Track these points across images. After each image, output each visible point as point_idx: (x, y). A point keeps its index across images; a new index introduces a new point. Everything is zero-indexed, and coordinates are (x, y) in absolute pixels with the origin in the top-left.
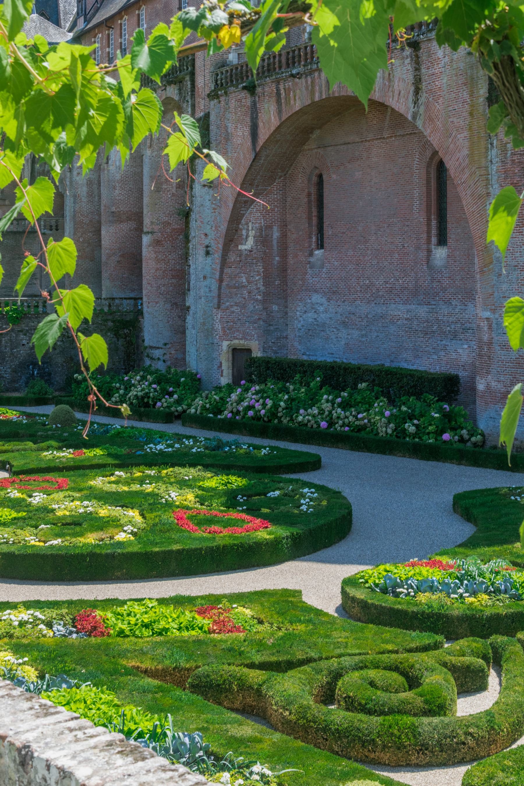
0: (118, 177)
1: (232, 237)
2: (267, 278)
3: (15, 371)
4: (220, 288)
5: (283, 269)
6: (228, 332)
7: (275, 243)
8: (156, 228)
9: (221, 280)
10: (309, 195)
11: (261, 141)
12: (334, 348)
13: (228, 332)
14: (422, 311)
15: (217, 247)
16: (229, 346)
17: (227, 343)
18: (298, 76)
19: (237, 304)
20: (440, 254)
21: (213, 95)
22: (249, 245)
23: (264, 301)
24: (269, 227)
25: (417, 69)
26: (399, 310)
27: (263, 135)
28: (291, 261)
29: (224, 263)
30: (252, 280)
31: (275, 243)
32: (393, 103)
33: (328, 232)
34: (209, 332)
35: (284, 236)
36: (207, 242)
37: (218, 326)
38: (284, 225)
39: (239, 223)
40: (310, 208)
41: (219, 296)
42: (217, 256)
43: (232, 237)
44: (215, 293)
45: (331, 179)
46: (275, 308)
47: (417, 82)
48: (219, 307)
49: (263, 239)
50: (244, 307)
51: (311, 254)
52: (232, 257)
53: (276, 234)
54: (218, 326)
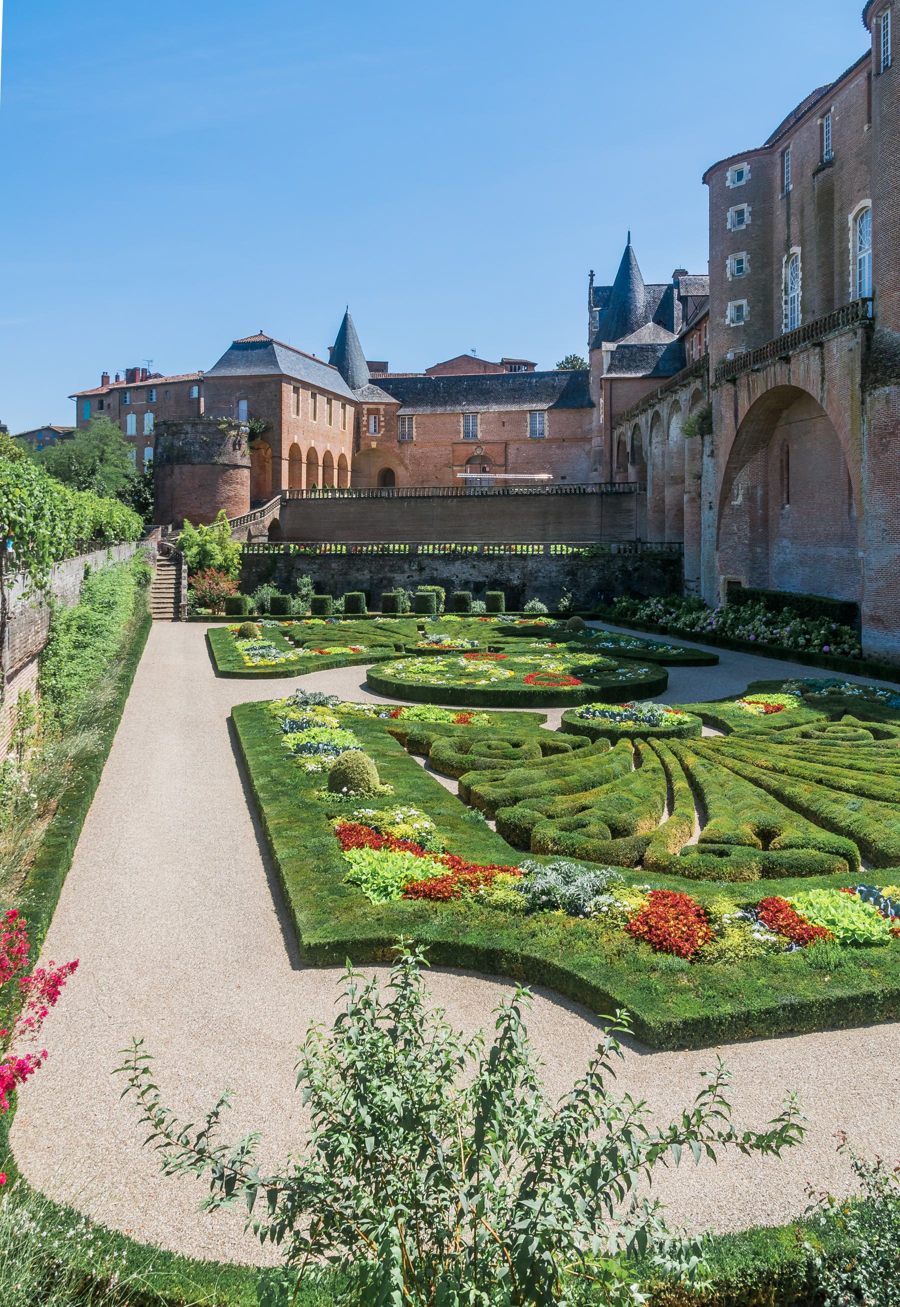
0: (675, 450)
1: (726, 495)
2: (753, 527)
3: (587, 596)
4: (718, 534)
5: (765, 520)
6: (724, 569)
7: (759, 499)
8: (692, 488)
9: (719, 529)
10: (782, 461)
11: (740, 421)
12: (794, 584)
13: (724, 569)
15: (716, 503)
16: (725, 580)
17: (722, 577)
18: (758, 370)
19: (730, 547)
22: (738, 501)
23: (750, 545)
24: (755, 487)
25: (823, 363)
27: (741, 417)
28: (771, 514)
29: (720, 515)
30: (741, 528)
31: (759, 499)
33: (792, 490)
34: (711, 569)
35: (766, 493)
36: (710, 499)
37: (717, 564)
38: (766, 485)
39: (731, 484)
40: (782, 471)
41: (718, 540)
42: (716, 509)
43: (726, 495)
44: (715, 539)
45: (794, 448)
46: (759, 550)
47: (823, 372)
48: (717, 549)
49: (750, 497)
50: (735, 549)
51: (783, 508)
52: (727, 511)
53: (760, 492)
54: (717, 564)
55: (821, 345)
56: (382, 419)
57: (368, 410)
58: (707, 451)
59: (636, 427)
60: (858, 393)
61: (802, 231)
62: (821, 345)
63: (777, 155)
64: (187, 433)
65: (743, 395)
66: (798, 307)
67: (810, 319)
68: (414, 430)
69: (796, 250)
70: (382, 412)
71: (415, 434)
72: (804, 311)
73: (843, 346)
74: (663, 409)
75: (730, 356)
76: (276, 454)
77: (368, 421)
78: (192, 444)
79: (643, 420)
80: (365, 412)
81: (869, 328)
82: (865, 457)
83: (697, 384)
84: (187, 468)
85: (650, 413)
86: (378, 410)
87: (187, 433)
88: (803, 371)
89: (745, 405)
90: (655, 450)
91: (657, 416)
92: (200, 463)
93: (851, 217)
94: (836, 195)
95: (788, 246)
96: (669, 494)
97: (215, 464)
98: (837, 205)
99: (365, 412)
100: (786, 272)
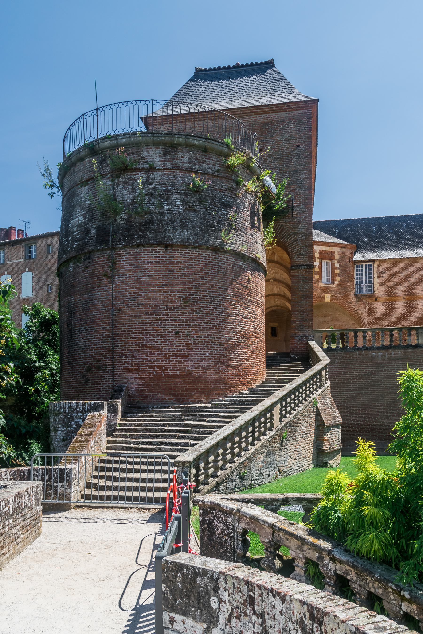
56: (337, 265)
57: (321, 252)
64: (152, 169)
68: (376, 280)
70: (337, 257)
71: (376, 285)
76: (301, 261)
77: (320, 267)
78: (166, 196)
80: (317, 255)
84: (151, 257)
86: (332, 253)
87: (152, 169)
92: (184, 245)
97: (218, 250)
99: (317, 255)
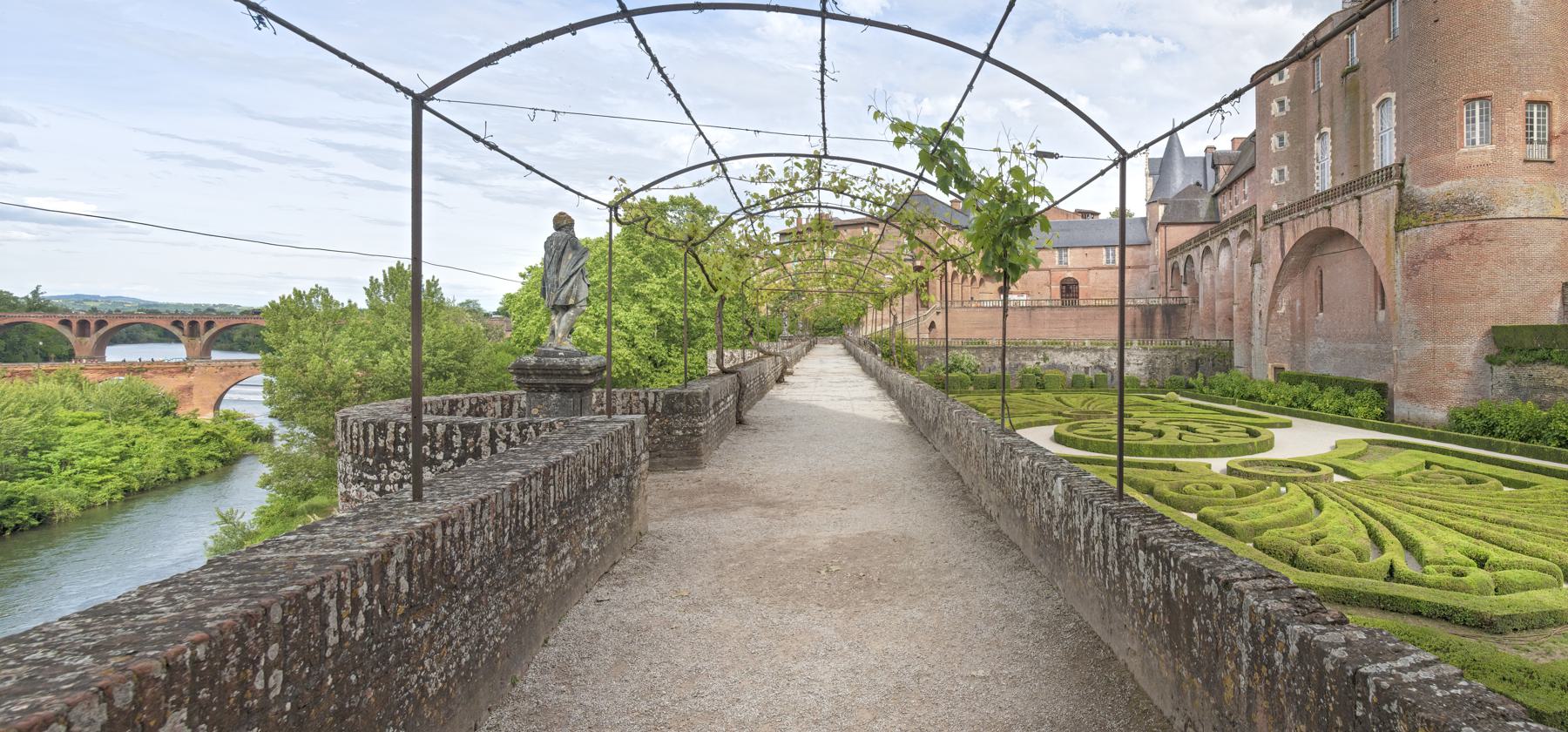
1: (1273, 306)
2: (1293, 328)
5: (1303, 324)
12: (1328, 369)
14: (1373, 347)
20: (1382, 315)
21: (1263, 229)
26: (1360, 346)
29: (1269, 320)
30: (1285, 330)
32: (1348, 230)
38: (1303, 300)
43: (1273, 306)
45: (1326, 273)
49: (1291, 307)
53: (1298, 304)
55: (1359, 198)
58: (1258, 274)
59: (1189, 257)
60: (1392, 233)
61: (1332, 117)
62: (1359, 198)
63: (1310, 61)
65: (1289, 234)
66: (1328, 171)
67: (1341, 181)
69: (1327, 129)
72: (1333, 174)
73: (1381, 200)
74: (1214, 245)
75: (1275, 207)
79: (1195, 254)
81: (1401, 186)
82: (1399, 278)
83: (1246, 227)
85: (1202, 248)
88: (1343, 217)
89: (1289, 243)
90: (1204, 273)
91: (1208, 250)
93: (1374, 106)
94: (1361, 90)
95: (1319, 126)
96: (1219, 305)
98: (1362, 97)
100: (1317, 146)
